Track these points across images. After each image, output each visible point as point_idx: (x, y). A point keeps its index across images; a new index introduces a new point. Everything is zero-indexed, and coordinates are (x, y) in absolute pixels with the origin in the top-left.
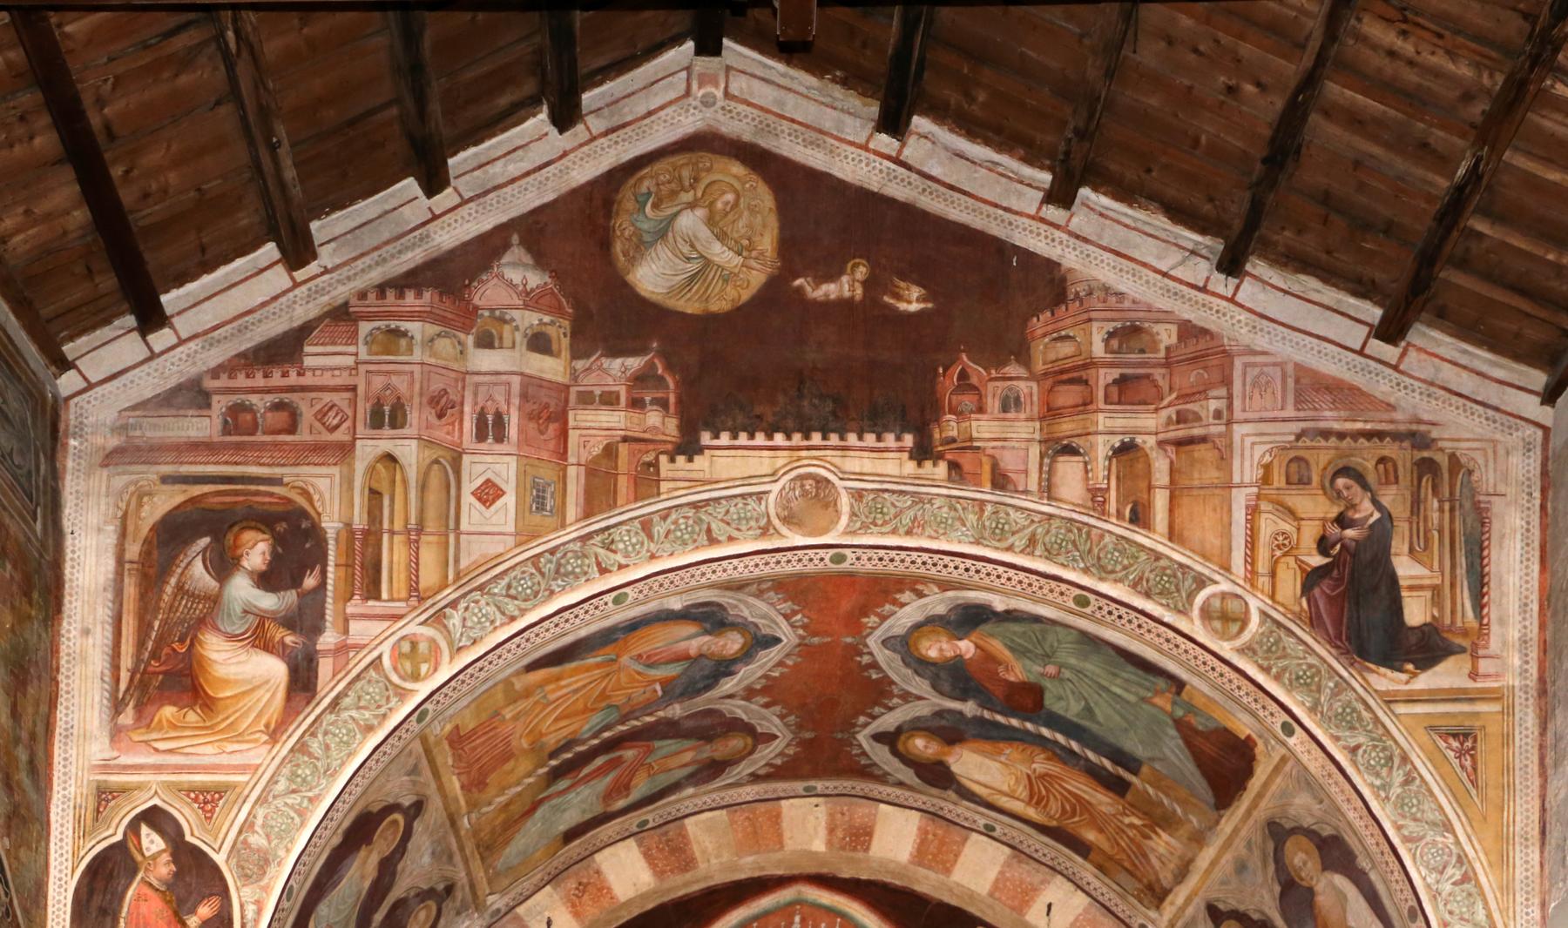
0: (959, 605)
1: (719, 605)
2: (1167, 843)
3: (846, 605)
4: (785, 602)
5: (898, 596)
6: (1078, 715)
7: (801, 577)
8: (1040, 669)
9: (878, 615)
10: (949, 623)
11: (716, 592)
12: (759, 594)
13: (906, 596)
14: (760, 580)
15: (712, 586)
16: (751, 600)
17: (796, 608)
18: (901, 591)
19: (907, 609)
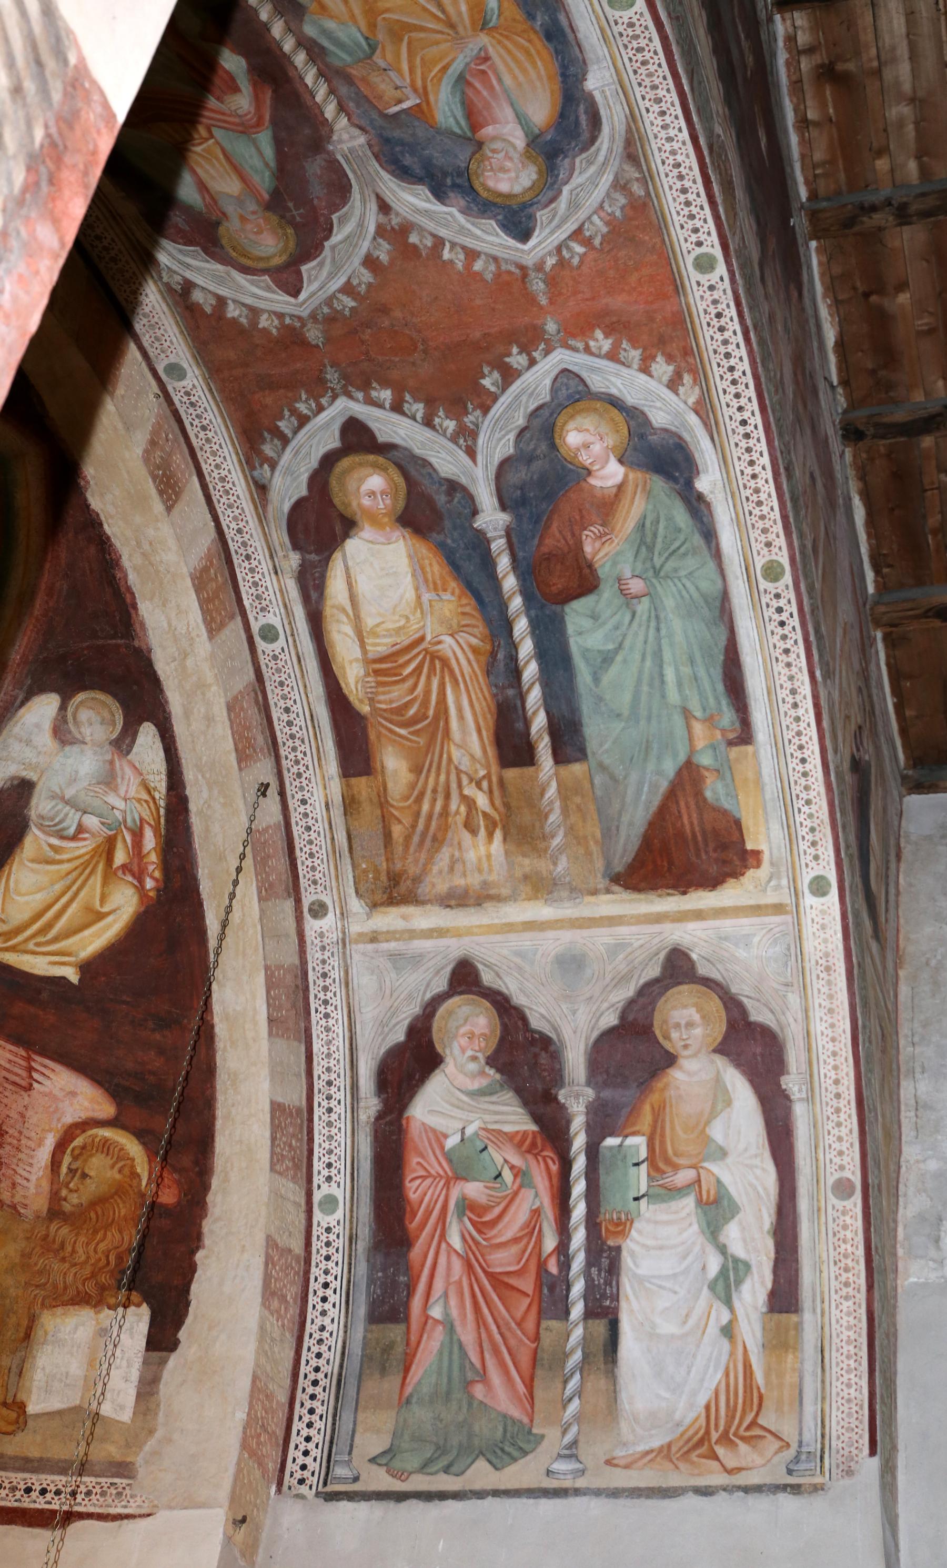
0: (680, 438)
1: (593, 139)
2: (489, 856)
3: (617, 302)
4: (607, 223)
5: (659, 358)
6: (585, 652)
7: (660, 227)
8: (628, 574)
9: (616, 347)
10: (642, 436)
11: (620, 128)
12: (620, 185)
13: (663, 368)
14: (648, 177)
15: (633, 118)
16: (607, 180)
17: (597, 242)
18: (670, 359)
19: (643, 377)
